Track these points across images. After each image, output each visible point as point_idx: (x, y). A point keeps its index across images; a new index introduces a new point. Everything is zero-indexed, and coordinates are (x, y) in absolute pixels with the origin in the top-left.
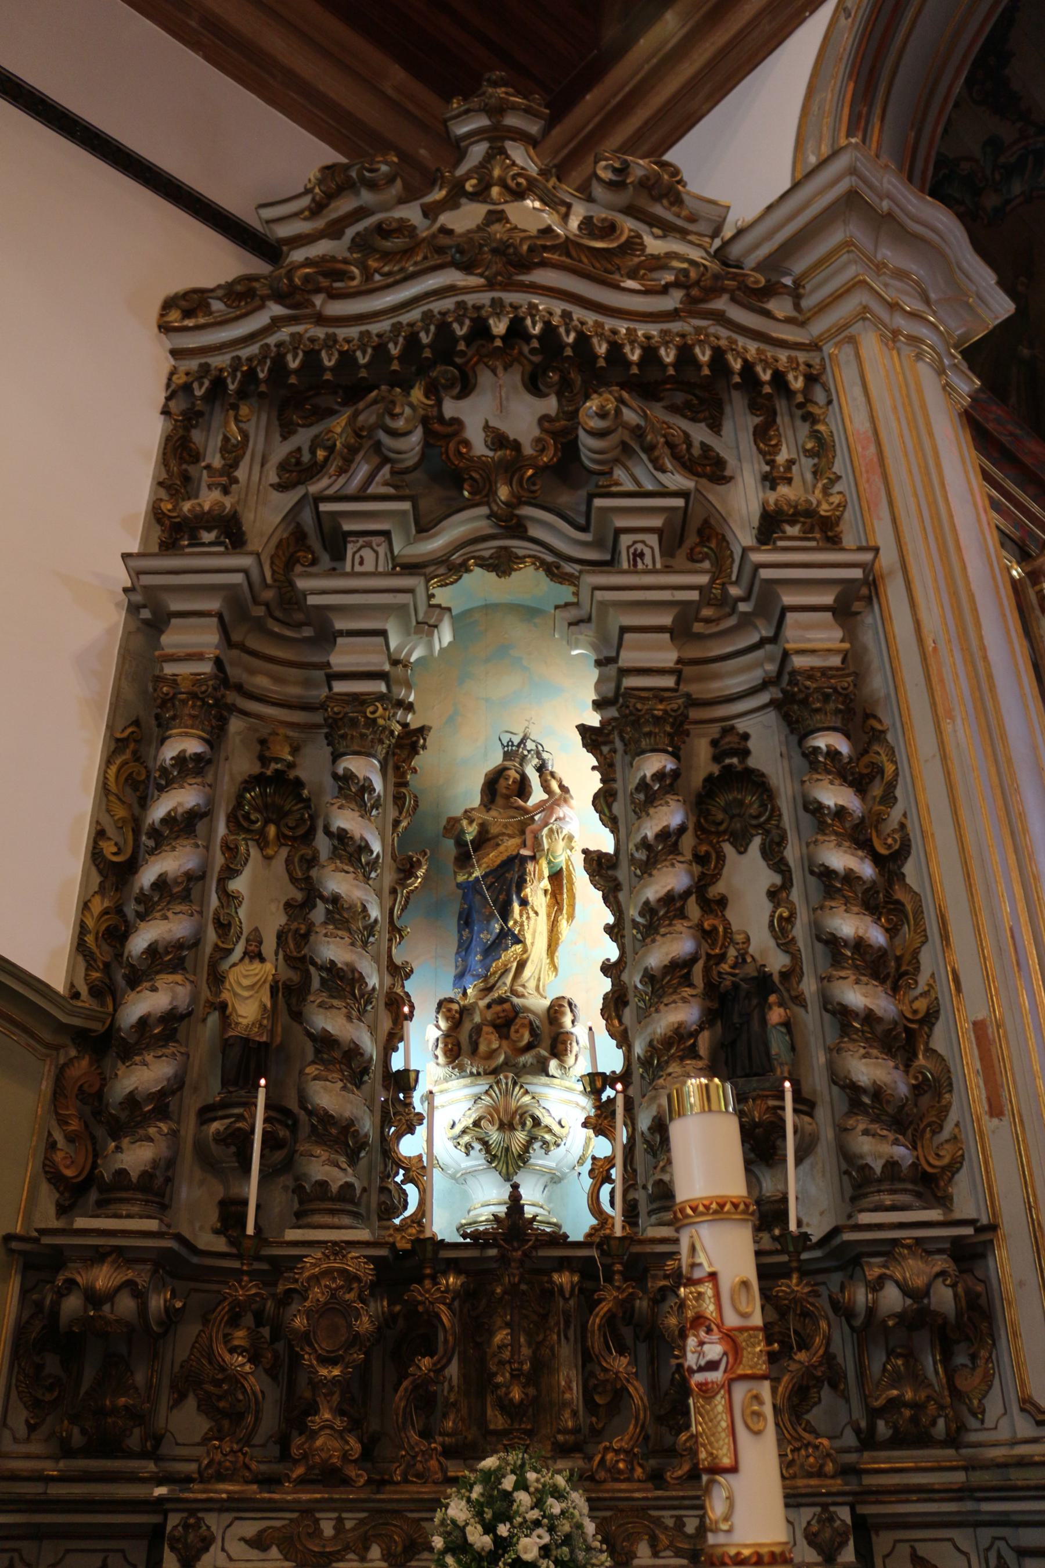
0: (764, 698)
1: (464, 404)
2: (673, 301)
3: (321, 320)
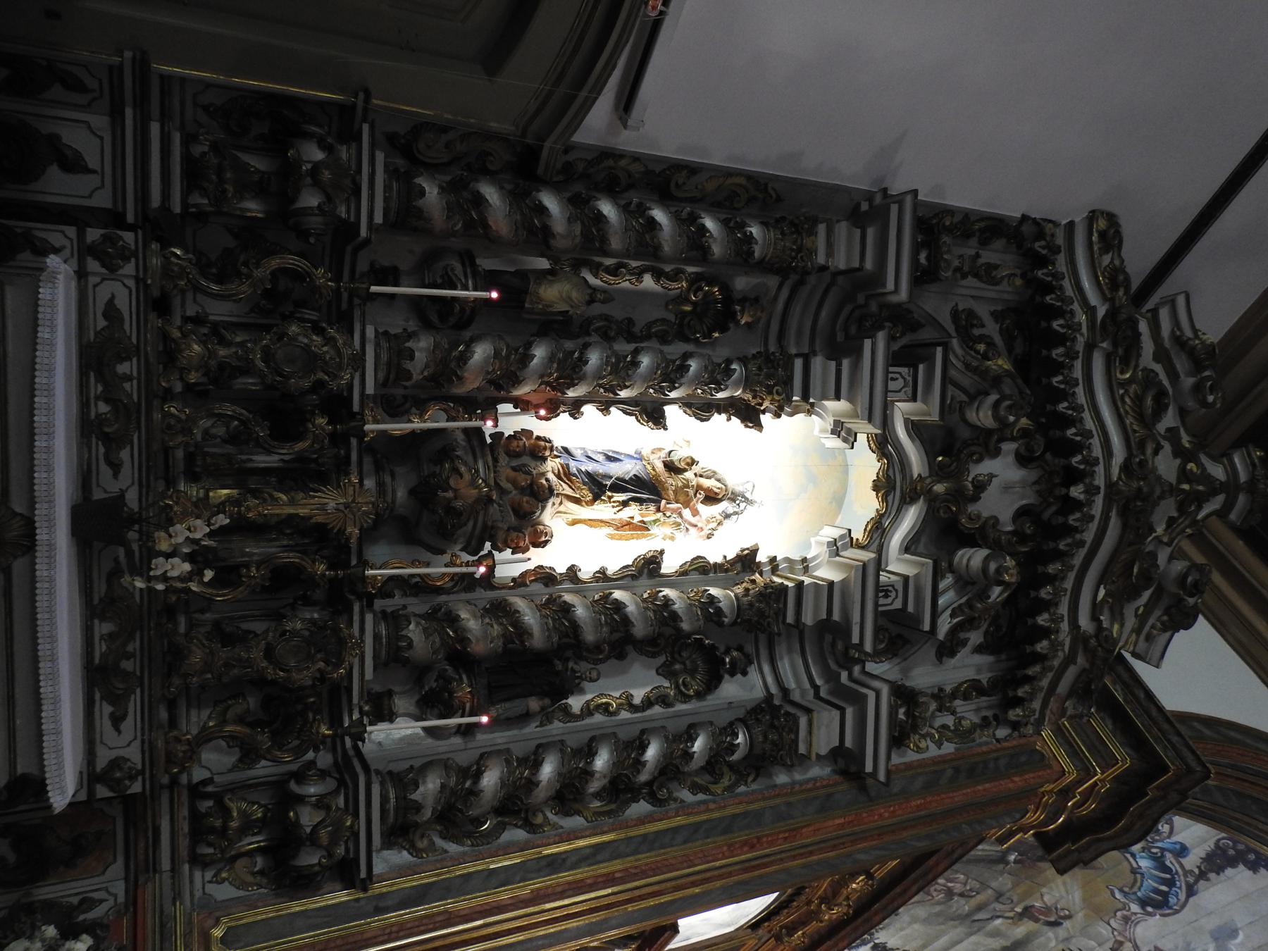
0: (774, 689)
1: (1011, 459)
2: (1084, 622)
3: (1090, 347)
